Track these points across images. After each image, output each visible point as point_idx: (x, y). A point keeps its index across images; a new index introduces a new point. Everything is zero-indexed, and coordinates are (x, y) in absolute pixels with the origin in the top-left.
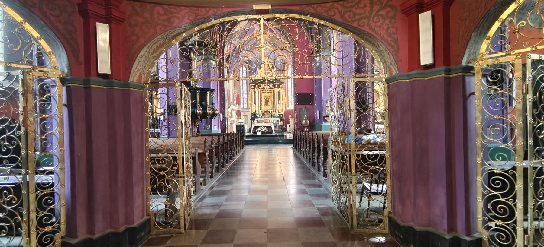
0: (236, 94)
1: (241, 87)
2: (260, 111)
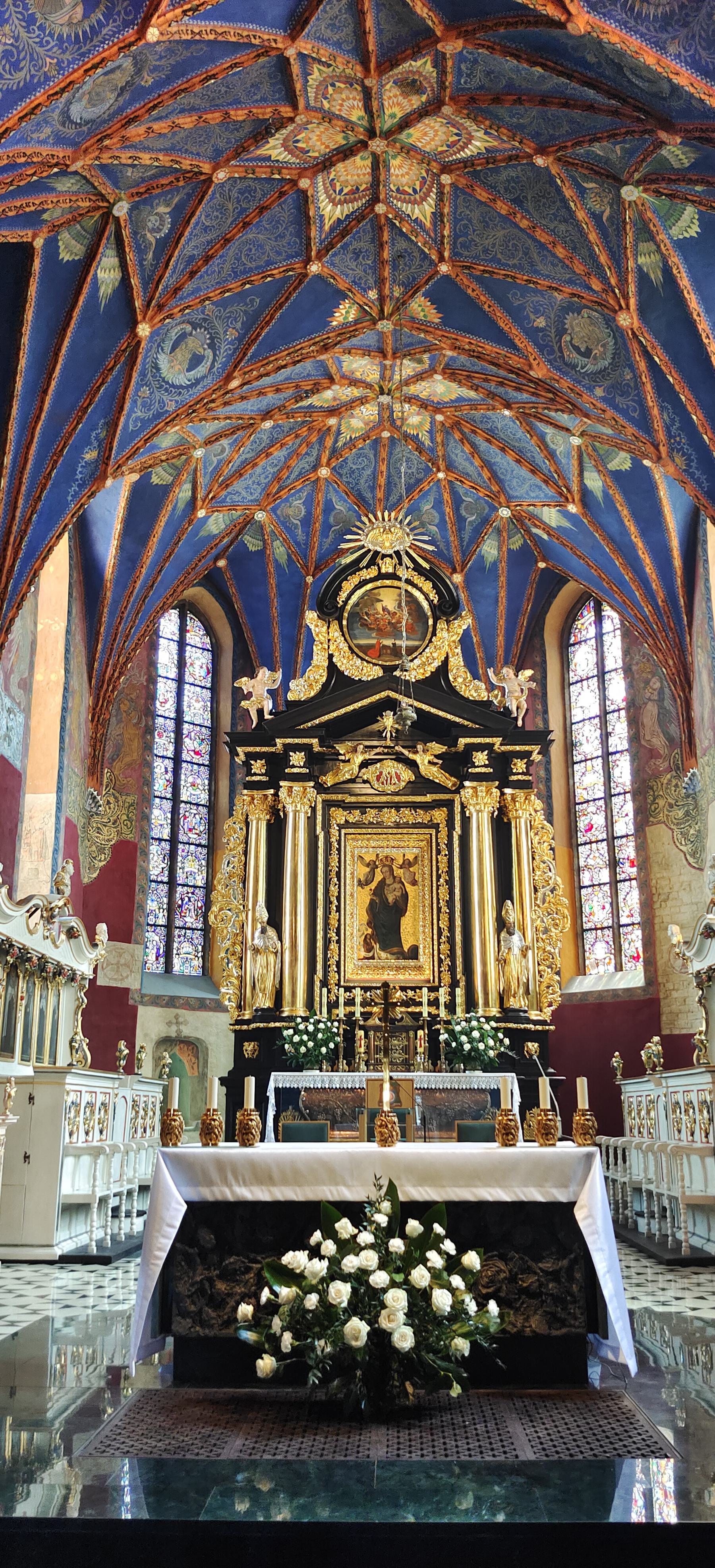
0: (109, 836)
1: (161, 784)
2: (322, 996)
